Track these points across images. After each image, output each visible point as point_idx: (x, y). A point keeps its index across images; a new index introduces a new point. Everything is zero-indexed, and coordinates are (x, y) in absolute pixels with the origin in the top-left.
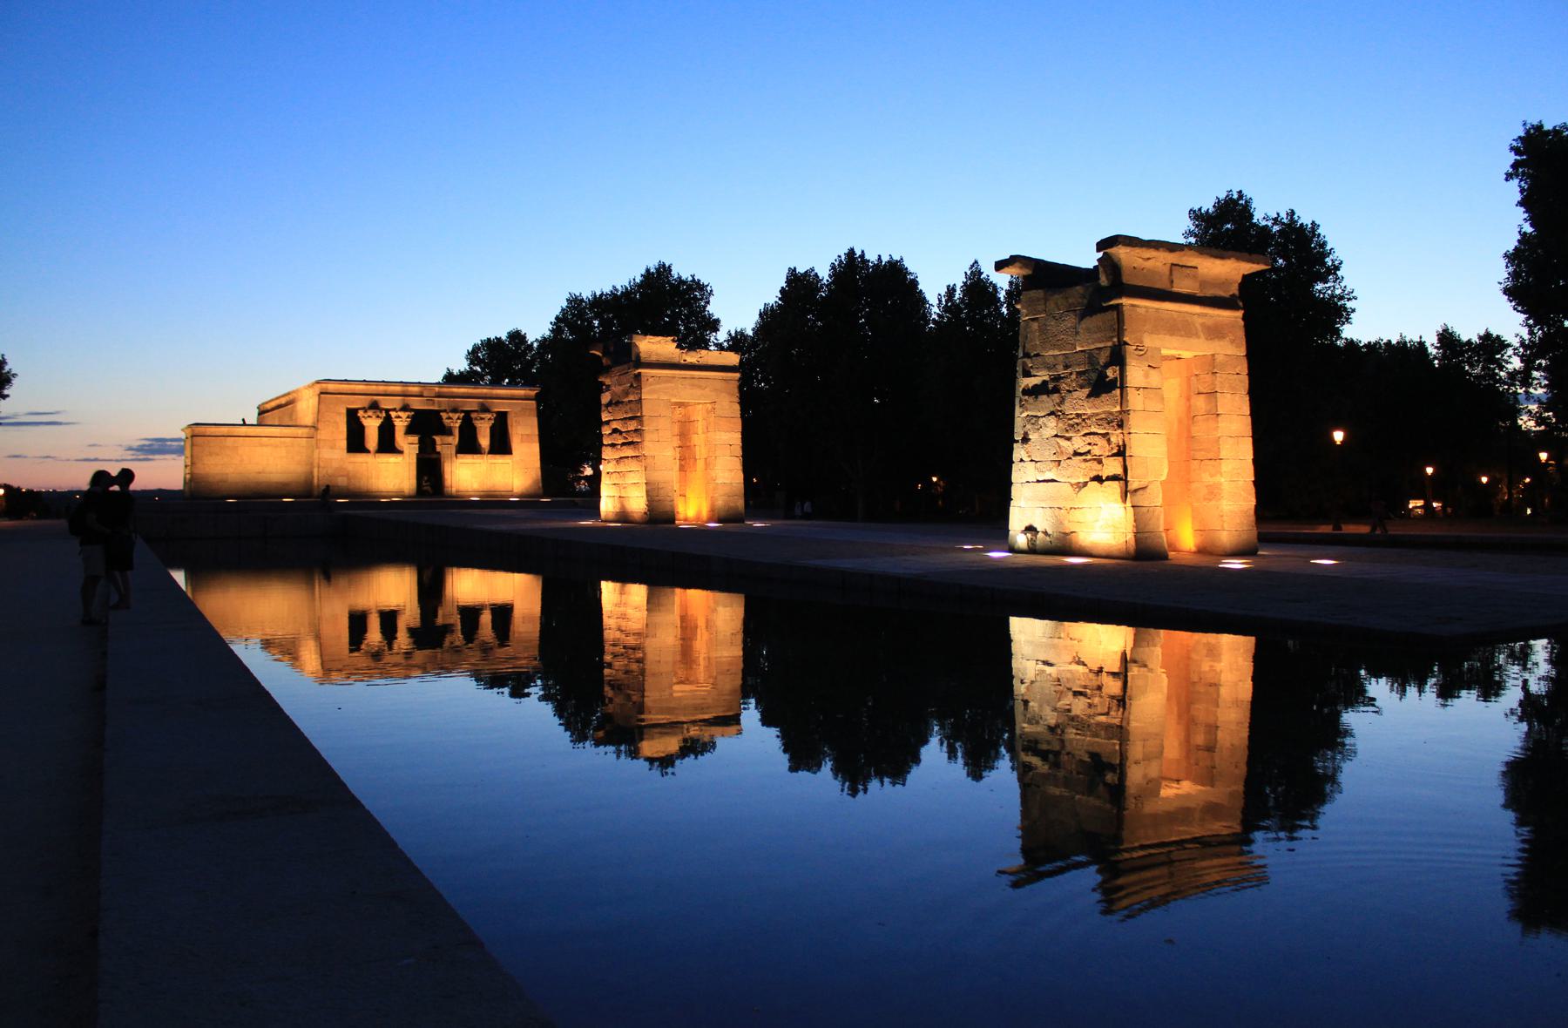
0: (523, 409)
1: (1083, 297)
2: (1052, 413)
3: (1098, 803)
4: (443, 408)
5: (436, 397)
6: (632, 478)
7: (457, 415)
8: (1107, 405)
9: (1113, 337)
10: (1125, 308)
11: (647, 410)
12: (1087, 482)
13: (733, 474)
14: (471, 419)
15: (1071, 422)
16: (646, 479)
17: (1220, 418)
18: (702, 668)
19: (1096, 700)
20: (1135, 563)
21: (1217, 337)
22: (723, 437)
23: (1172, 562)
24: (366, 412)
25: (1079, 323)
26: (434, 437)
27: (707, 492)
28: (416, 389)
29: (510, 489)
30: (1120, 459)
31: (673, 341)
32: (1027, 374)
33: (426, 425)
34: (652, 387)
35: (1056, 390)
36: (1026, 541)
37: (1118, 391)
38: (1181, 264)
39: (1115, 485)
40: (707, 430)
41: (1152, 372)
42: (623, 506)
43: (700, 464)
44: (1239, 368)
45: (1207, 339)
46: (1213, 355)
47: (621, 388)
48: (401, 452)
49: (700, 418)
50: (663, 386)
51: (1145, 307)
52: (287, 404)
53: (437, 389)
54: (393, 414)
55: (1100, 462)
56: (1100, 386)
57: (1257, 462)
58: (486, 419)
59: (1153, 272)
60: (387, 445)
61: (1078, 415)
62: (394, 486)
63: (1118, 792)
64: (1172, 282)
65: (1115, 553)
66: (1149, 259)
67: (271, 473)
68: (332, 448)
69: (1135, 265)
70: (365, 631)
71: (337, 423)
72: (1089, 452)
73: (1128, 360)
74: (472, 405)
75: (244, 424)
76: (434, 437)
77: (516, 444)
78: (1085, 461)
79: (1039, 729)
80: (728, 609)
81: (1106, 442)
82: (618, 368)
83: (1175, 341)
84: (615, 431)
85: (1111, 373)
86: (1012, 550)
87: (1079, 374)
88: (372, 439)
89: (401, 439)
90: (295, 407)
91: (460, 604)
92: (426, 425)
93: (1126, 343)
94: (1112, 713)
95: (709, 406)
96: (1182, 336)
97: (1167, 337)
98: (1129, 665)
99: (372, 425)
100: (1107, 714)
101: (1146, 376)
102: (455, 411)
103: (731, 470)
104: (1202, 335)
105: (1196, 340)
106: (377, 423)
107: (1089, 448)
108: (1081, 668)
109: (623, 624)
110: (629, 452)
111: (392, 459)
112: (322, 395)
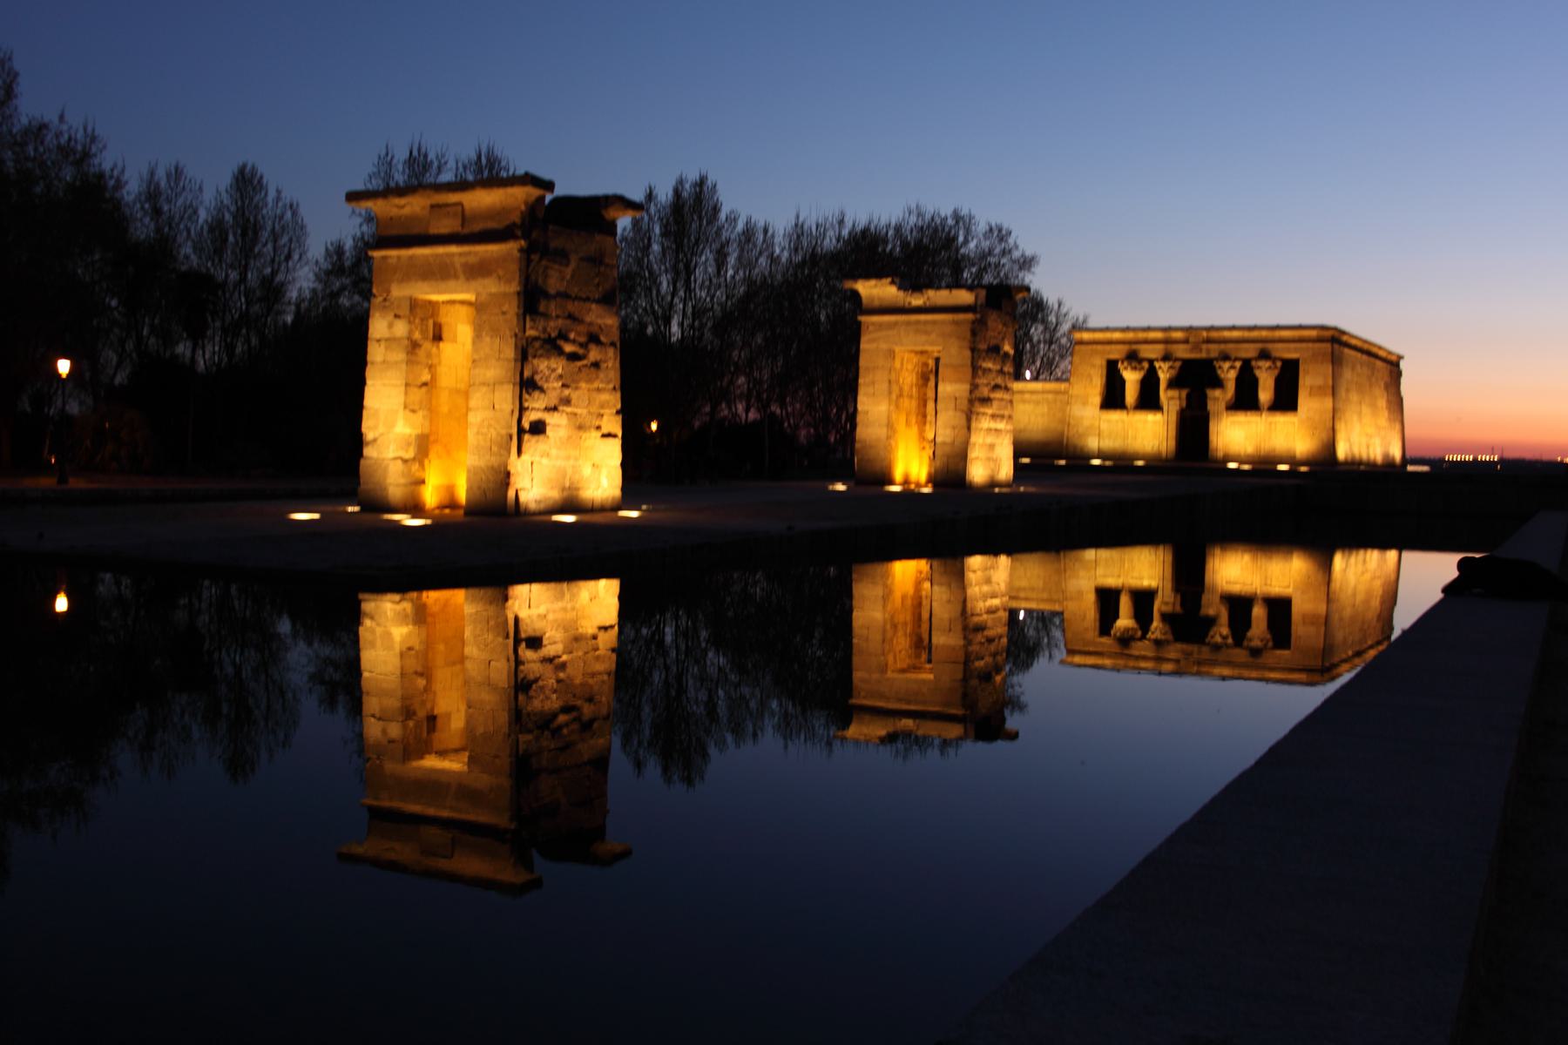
4: (1213, 355)
7: (1226, 365)
13: (956, 431)
28: (1178, 335)
31: (893, 283)
45: (468, 279)
51: (399, 258)
54: (1157, 365)
58: (1264, 369)
59: (413, 219)
60: (1149, 400)
62: (1153, 447)
69: (392, 214)
70: (1117, 617)
74: (1249, 351)
77: (1304, 401)
88: (1131, 394)
89: (1164, 395)
93: (375, 296)
99: (1132, 378)
101: (390, 326)
102: (1226, 357)
103: (954, 428)
104: (462, 277)
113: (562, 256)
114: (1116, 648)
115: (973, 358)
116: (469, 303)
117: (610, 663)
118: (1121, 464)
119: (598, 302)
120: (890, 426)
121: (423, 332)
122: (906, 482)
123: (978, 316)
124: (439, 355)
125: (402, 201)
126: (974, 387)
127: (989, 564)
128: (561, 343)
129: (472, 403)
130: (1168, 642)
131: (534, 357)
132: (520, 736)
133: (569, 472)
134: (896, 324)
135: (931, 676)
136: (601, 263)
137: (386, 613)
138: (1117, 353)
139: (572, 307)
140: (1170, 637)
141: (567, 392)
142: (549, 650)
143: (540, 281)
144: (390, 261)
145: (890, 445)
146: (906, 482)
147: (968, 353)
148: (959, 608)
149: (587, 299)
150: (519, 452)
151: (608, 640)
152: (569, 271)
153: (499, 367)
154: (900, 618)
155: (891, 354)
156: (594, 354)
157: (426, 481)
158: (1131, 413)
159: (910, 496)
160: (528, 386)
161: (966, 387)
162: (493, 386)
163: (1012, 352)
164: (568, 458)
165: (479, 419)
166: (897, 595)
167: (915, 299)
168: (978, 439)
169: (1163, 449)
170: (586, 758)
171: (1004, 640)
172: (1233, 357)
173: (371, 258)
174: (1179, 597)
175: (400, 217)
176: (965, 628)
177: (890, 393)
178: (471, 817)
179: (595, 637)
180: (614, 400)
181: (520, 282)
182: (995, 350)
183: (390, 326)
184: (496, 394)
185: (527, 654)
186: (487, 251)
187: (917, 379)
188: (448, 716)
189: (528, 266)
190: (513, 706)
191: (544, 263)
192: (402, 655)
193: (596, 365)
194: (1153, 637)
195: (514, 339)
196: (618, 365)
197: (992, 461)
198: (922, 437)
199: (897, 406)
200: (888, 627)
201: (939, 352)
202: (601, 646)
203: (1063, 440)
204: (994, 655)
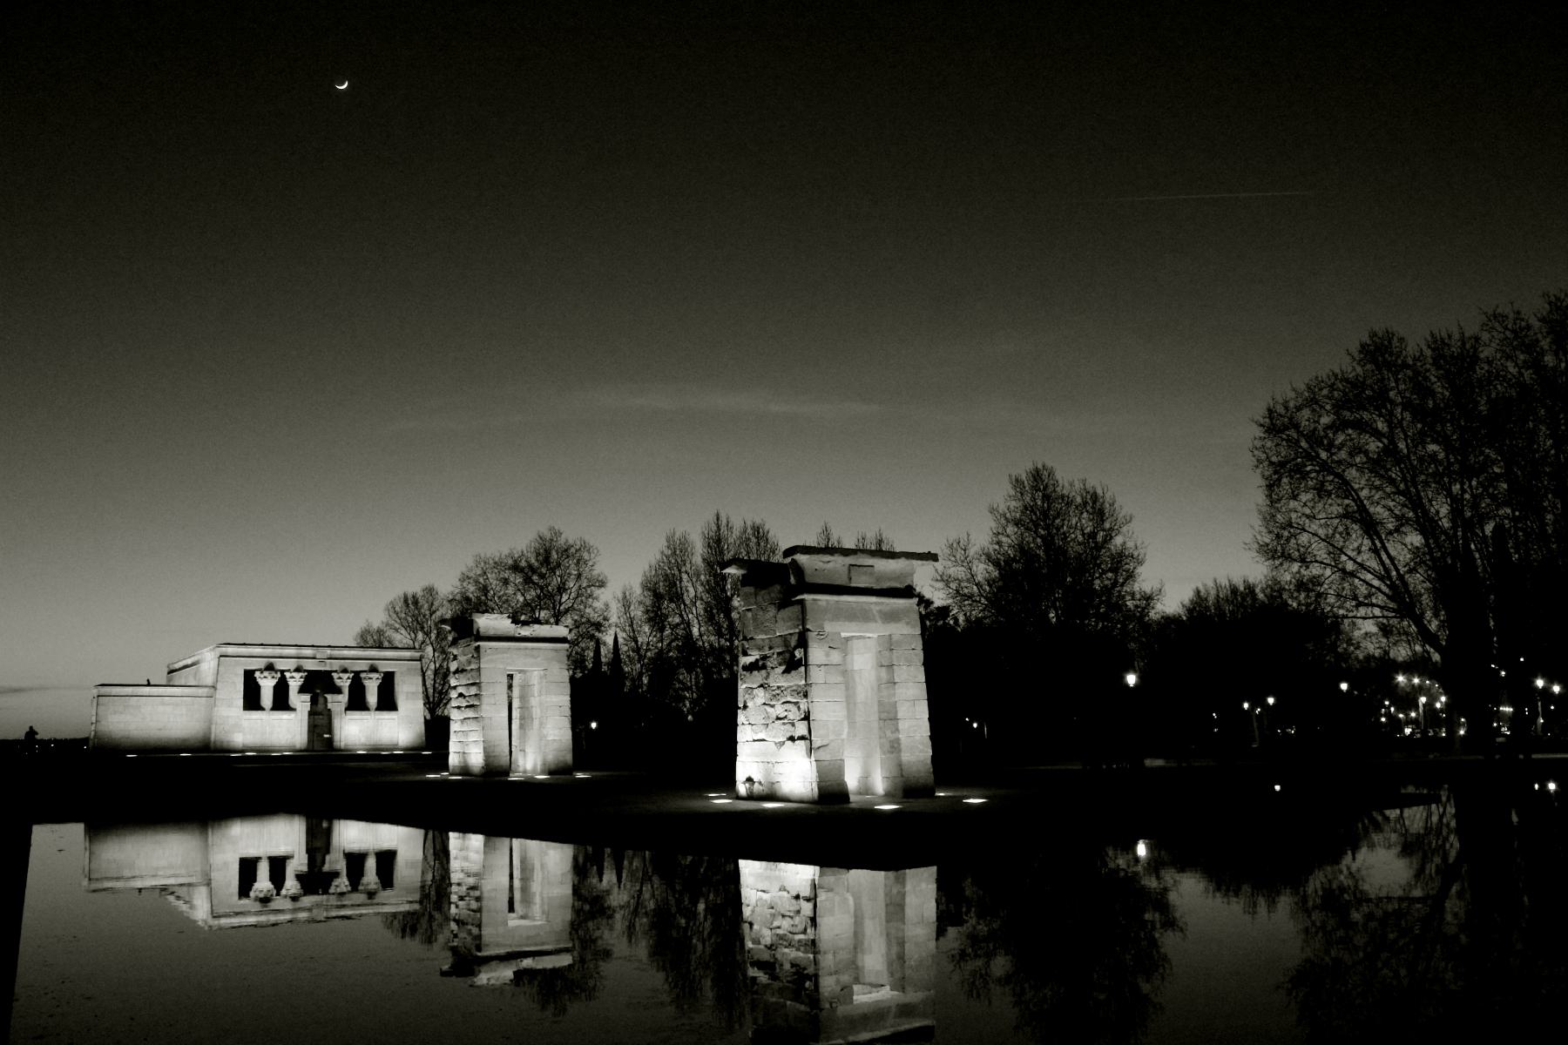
0: (408, 669)
1: (780, 592)
2: (761, 686)
3: (803, 1008)
6: (473, 737)
7: (345, 676)
8: (796, 679)
9: (798, 625)
10: (807, 602)
11: (483, 679)
12: (784, 742)
13: (562, 731)
14: (361, 678)
15: (774, 693)
16: (483, 737)
17: (897, 686)
18: (538, 906)
19: (797, 920)
20: (819, 807)
22: (554, 700)
23: (852, 806)
24: (262, 673)
25: (779, 610)
26: (326, 695)
27: (540, 748)
28: (308, 652)
29: (395, 742)
30: (806, 722)
31: (509, 617)
32: (745, 654)
33: (318, 684)
34: (489, 657)
35: (764, 667)
36: (745, 790)
37: (803, 669)
38: (858, 564)
39: (802, 742)
40: (540, 696)
41: (832, 650)
42: (465, 761)
43: (536, 723)
45: (883, 623)
46: (890, 635)
47: (465, 657)
48: (294, 710)
49: (536, 683)
50: (500, 656)
51: (827, 600)
52: (193, 664)
53: (329, 651)
54: (287, 675)
55: (793, 725)
56: (792, 665)
57: (932, 719)
60: (281, 702)
61: (779, 687)
63: (814, 999)
64: (850, 579)
65: (806, 799)
68: (229, 706)
71: (234, 683)
72: (786, 717)
73: (810, 644)
75: (149, 685)
76: (326, 695)
78: (784, 724)
79: (762, 947)
81: (796, 709)
82: (463, 641)
83: (853, 625)
84: (461, 695)
85: (798, 654)
86: (739, 798)
87: (779, 654)
88: (267, 697)
90: (198, 669)
91: (346, 852)
92: (318, 684)
93: (809, 630)
94: (809, 931)
95: (542, 672)
96: (860, 621)
97: (847, 623)
98: (818, 891)
99: (267, 684)
100: (804, 932)
101: (827, 655)
102: (345, 671)
103: (560, 729)
104: (880, 622)
105: (874, 624)
106: (274, 682)
107: (786, 713)
108: (785, 894)
109: (466, 864)
110: (470, 713)
111: (284, 716)
112: (222, 658)
114: (257, 906)
125: (827, 558)
130: (301, 896)
144: (820, 603)
167: (526, 630)
172: (349, 670)
175: (824, 570)
184: (917, 708)
203: (209, 738)
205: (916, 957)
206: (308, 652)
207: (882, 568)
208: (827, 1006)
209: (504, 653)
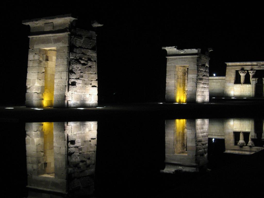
5: (262, 65)
10: (30, 39)
13: (193, 88)
21: (58, 42)
22: (191, 76)
31: (175, 47)
34: (170, 62)
38: (47, 23)
44: (65, 50)
45: (54, 43)
50: (173, 61)
51: (36, 38)
53: (262, 63)
54: (249, 71)
60: (247, 81)
62: (248, 94)
66: (38, 24)
67: (216, 90)
68: (230, 83)
70: (239, 140)
71: (231, 75)
80: (190, 130)
88: (242, 79)
89: (251, 80)
96: (46, 44)
97: (42, 45)
99: (242, 75)
101: (34, 57)
104: (53, 42)
111: (248, 86)
113: (80, 36)
115: (197, 67)
116: (54, 50)
117: (94, 148)
118: (240, 99)
119: (90, 49)
120: (175, 87)
121: (43, 58)
122: (180, 102)
123: (199, 56)
124: (47, 65)
126: (198, 75)
127: (203, 123)
128: (79, 60)
129: (56, 77)
130: (253, 146)
131: (73, 64)
132: (69, 169)
133: (83, 96)
134: (176, 58)
135: (187, 155)
136: (92, 39)
137: (32, 134)
138: (238, 68)
139: (83, 51)
140: (254, 145)
141: (82, 74)
142: (77, 144)
143: (74, 43)
144: (34, 39)
145: (175, 92)
146: (180, 102)
147: (196, 66)
148: (194, 135)
149: (88, 49)
150: (68, 91)
151: (94, 142)
152: (82, 41)
153: (63, 67)
154: (178, 139)
155: (175, 67)
156: (90, 64)
157: (44, 99)
158: (242, 85)
159: (180, 105)
160: (71, 72)
161: (196, 75)
162: (61, 72)
163: (208, 66)
164: (82, 92)
165: (57, 81)
166: (178, 132)
168: (199, 90)
169: (251, 94)
170: (88, 175)
171: (207, 145)
173: (29, 38)
174: (256, 135)
176: (196, 141)
177: (175, 78)
178: (56, 191)
179: (90, 141)
180: (96, 77)
181: (68, 44)
182: (204, 65)
183: (34, 57)
184: (62, 74)
185: (72, 146)
186: (60, 35)
187: (183, 74)
188: (50, 163)
189: (70, 39)
190: (67, 160)
191: (75, 38)
192: (37, 146)
193: (90, 67)
194: (249, 145)
195: (67, 59)
196: (96, 67)
197: (204, 96)
198: (184, 90)
199: (177, 81)
200: (175, 141)
201: (188, 66)
202: (92, 144)
204: (204, 149)
205: (58, 166)
206: (255, 63)
207: (56, 23)
208: (29, 174)
209: (175, 60)
